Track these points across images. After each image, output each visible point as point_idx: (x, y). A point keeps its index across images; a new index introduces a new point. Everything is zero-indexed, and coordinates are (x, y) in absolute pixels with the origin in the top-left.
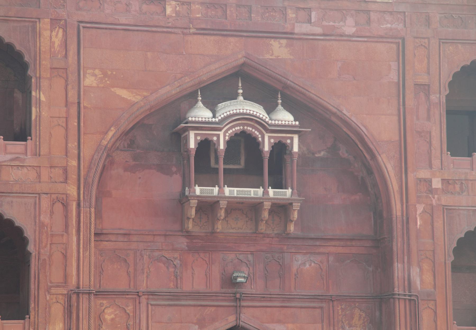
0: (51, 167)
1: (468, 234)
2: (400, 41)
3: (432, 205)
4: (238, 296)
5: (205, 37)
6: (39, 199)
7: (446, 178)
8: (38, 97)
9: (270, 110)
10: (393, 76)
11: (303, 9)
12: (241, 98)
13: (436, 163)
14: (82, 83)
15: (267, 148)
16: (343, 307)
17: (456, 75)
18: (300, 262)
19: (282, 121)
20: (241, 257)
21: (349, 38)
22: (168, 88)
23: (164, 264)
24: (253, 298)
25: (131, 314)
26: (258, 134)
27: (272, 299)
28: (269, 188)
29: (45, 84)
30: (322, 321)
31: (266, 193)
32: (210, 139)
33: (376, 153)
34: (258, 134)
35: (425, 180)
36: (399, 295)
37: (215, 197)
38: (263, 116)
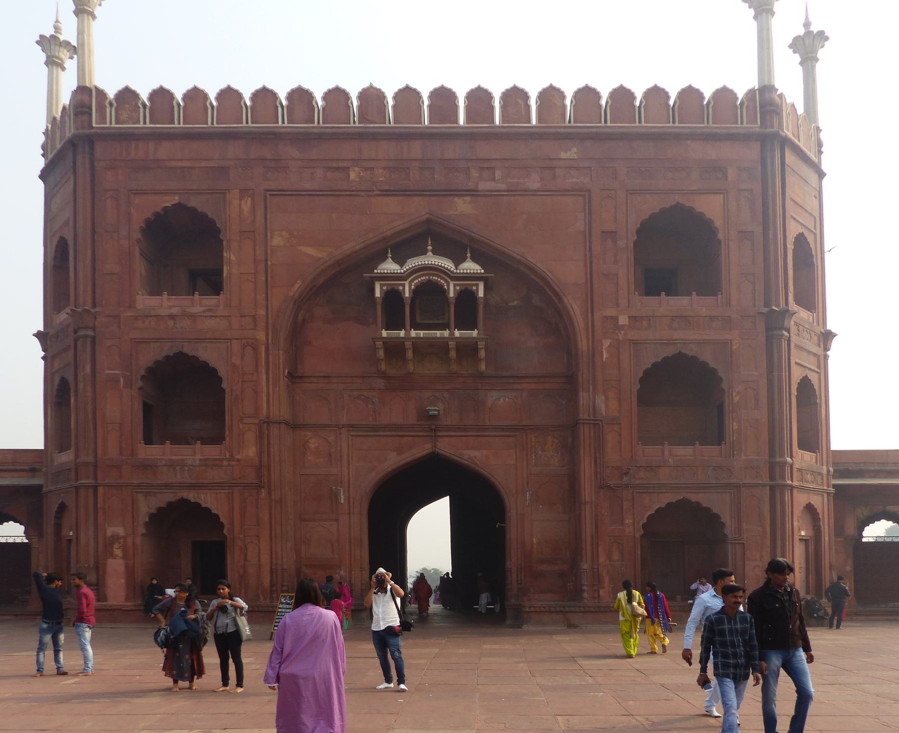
0: (242, 316)
1: (655, 365)
2: (587, 194)
4: (433, 427)
5: (389, 198)
6: (231, 344)
7: (634, 315)
8: (228, 257)
9: (458, 262)
10: (580, 226)
11: (487, 168)
14: (269, 243)
15: (452, 294)
16: (536, 434)
18: (494, 398)
19: (467, 270)
21: (534, 193)
24: (448, 428)
26: (443, 282)
27: (467, 430)
28: (455, 330)
31: (452, 334)
32: (396, 288)
33: (561, 294)
34: (443, 282)
36: (584, 420)
37: (402, 338)
38: (451, 267)
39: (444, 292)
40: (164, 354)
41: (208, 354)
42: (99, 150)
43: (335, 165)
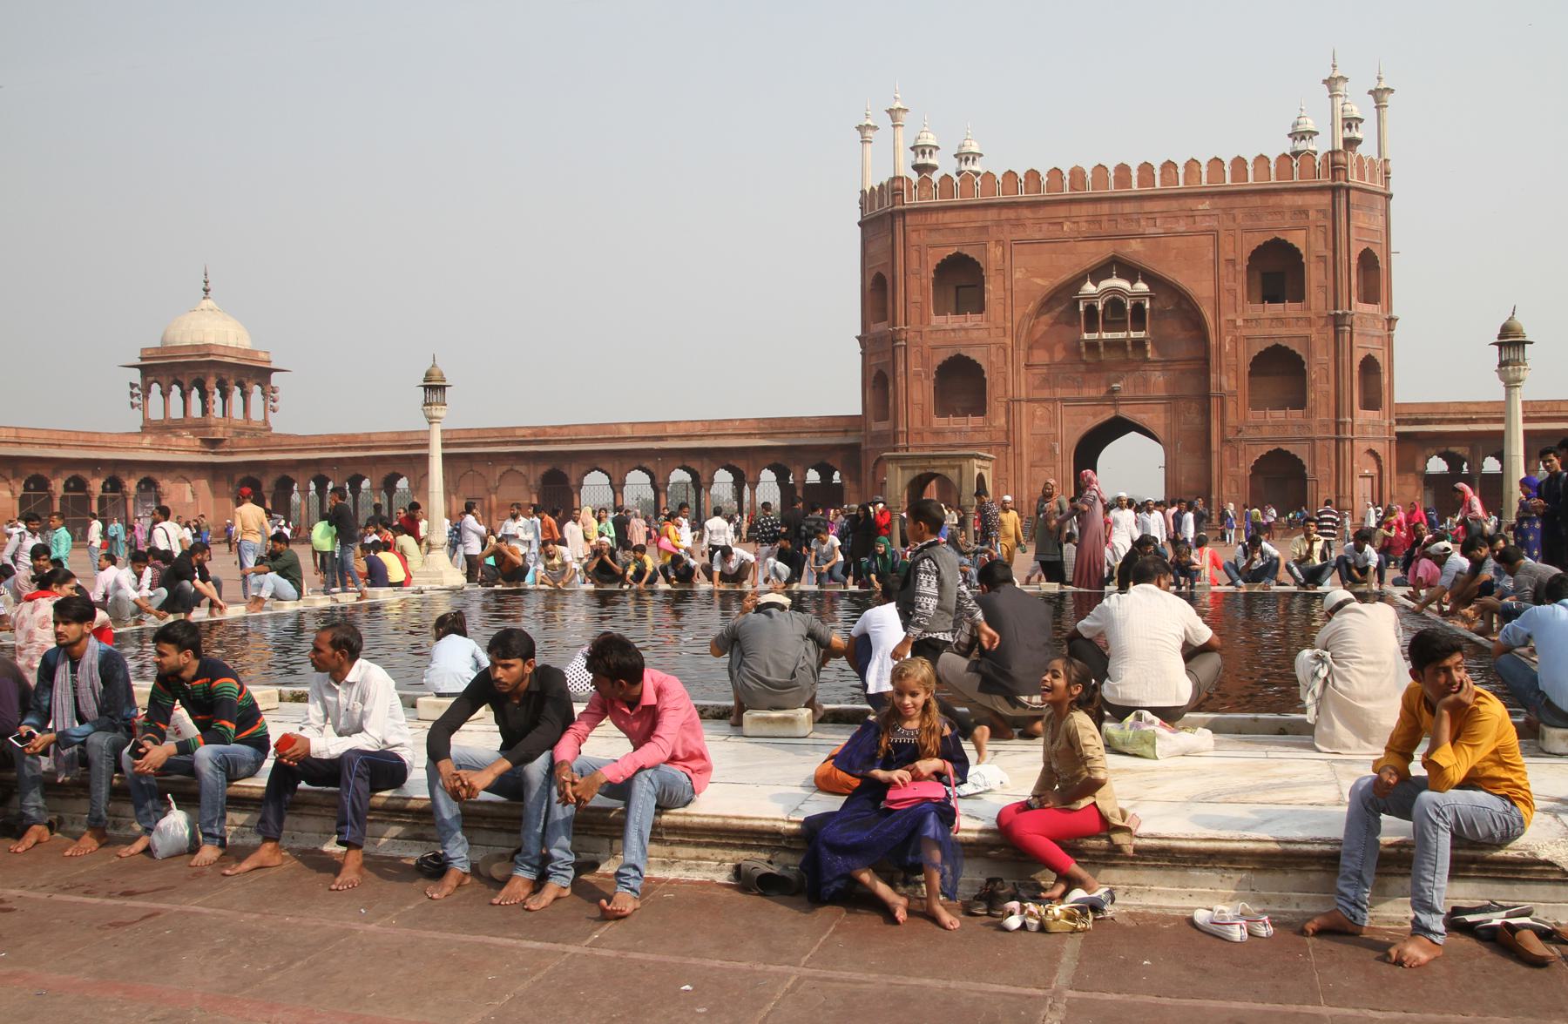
29: (992, 279)
41: (975, 355)
42: (908, 218)
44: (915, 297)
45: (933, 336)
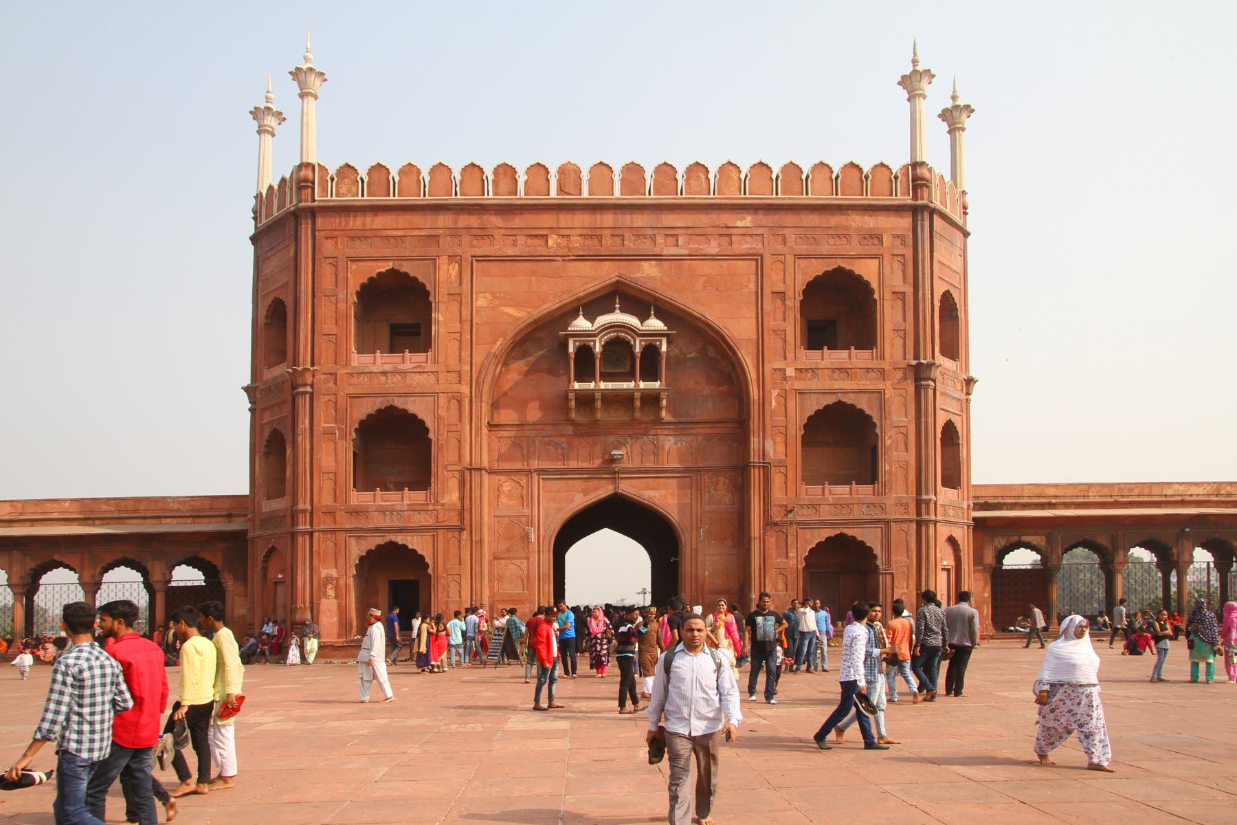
1: (818, 412)
2: (759, 258)
3: (786, 390)
9: (643, 318)
10: (752, 286)
11: (671, 235)
12: (618, 311)
13: (790, 355)
15: (638, 349)
17: (809, 284)
20: (620, 440)
22: (550, 304)
23: (553, 446)
25: (525, 486)
29: (442, 307)
30: (691, 488)
31: (637, 385)
35: (780, 369)
39: (629, 347)
40: (376, 408)
41: (417, 407)
42: (320, 222)
43: (534, 233)
44: (328, 326)
45: (354, 380)
